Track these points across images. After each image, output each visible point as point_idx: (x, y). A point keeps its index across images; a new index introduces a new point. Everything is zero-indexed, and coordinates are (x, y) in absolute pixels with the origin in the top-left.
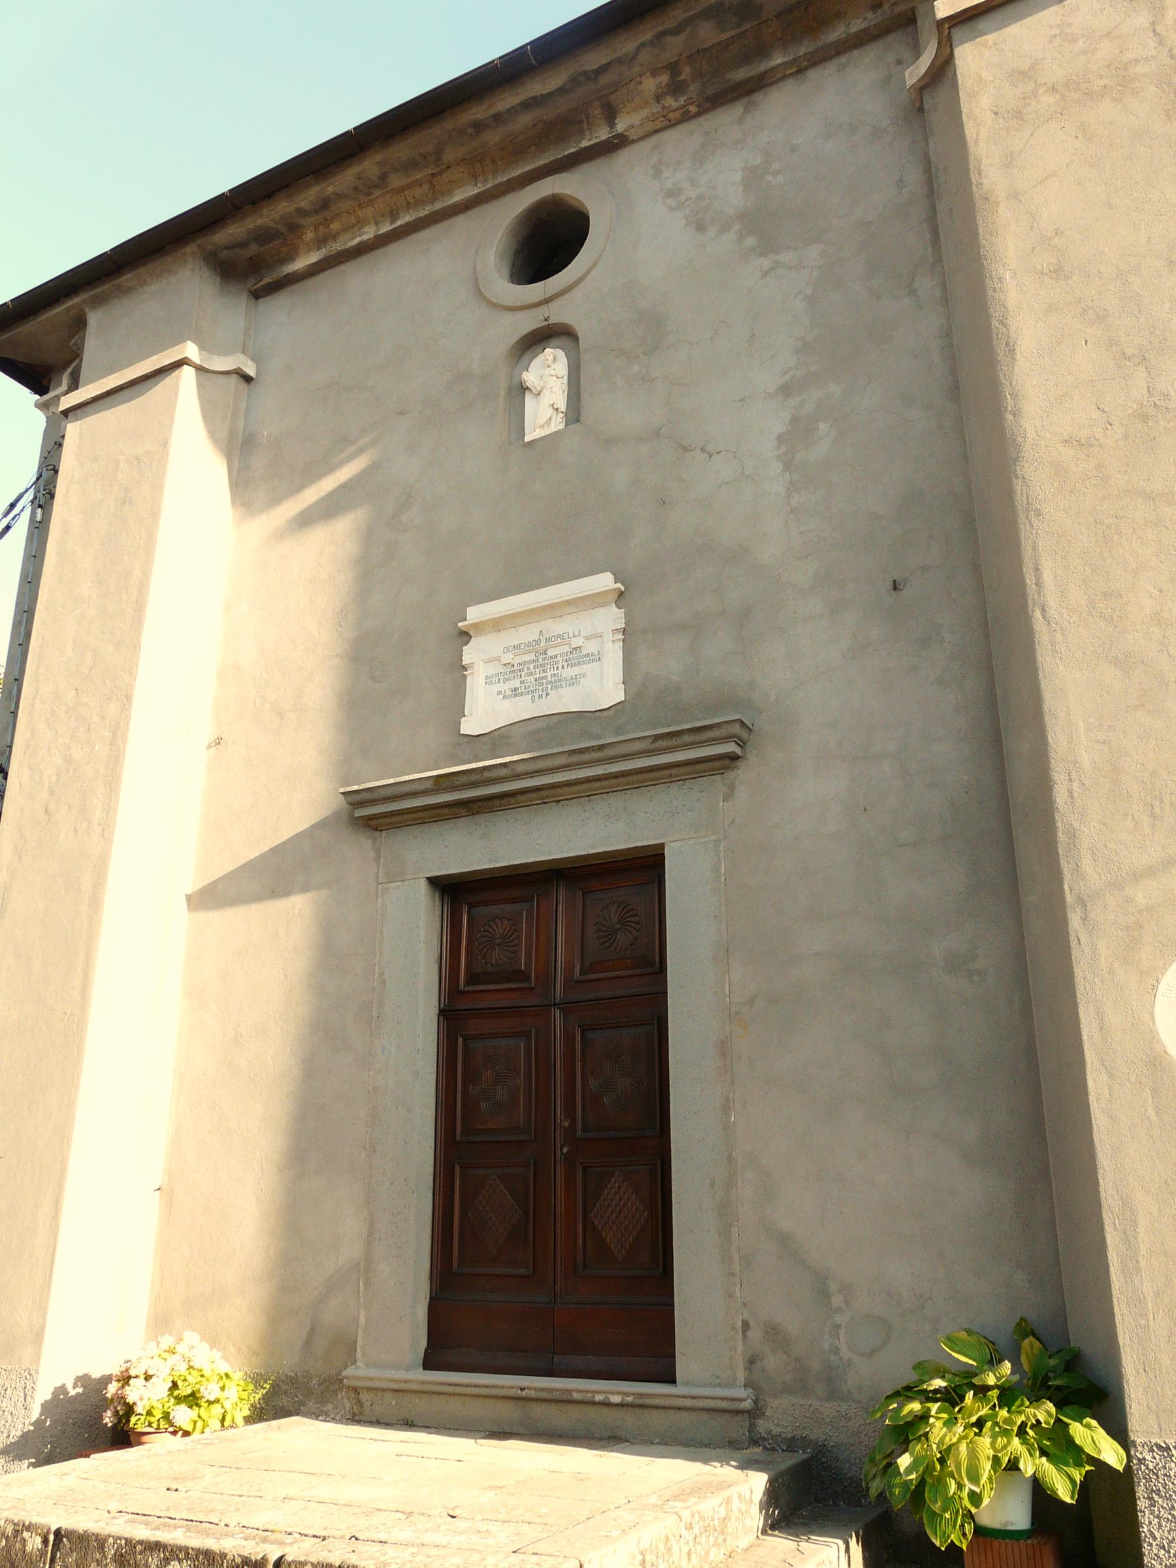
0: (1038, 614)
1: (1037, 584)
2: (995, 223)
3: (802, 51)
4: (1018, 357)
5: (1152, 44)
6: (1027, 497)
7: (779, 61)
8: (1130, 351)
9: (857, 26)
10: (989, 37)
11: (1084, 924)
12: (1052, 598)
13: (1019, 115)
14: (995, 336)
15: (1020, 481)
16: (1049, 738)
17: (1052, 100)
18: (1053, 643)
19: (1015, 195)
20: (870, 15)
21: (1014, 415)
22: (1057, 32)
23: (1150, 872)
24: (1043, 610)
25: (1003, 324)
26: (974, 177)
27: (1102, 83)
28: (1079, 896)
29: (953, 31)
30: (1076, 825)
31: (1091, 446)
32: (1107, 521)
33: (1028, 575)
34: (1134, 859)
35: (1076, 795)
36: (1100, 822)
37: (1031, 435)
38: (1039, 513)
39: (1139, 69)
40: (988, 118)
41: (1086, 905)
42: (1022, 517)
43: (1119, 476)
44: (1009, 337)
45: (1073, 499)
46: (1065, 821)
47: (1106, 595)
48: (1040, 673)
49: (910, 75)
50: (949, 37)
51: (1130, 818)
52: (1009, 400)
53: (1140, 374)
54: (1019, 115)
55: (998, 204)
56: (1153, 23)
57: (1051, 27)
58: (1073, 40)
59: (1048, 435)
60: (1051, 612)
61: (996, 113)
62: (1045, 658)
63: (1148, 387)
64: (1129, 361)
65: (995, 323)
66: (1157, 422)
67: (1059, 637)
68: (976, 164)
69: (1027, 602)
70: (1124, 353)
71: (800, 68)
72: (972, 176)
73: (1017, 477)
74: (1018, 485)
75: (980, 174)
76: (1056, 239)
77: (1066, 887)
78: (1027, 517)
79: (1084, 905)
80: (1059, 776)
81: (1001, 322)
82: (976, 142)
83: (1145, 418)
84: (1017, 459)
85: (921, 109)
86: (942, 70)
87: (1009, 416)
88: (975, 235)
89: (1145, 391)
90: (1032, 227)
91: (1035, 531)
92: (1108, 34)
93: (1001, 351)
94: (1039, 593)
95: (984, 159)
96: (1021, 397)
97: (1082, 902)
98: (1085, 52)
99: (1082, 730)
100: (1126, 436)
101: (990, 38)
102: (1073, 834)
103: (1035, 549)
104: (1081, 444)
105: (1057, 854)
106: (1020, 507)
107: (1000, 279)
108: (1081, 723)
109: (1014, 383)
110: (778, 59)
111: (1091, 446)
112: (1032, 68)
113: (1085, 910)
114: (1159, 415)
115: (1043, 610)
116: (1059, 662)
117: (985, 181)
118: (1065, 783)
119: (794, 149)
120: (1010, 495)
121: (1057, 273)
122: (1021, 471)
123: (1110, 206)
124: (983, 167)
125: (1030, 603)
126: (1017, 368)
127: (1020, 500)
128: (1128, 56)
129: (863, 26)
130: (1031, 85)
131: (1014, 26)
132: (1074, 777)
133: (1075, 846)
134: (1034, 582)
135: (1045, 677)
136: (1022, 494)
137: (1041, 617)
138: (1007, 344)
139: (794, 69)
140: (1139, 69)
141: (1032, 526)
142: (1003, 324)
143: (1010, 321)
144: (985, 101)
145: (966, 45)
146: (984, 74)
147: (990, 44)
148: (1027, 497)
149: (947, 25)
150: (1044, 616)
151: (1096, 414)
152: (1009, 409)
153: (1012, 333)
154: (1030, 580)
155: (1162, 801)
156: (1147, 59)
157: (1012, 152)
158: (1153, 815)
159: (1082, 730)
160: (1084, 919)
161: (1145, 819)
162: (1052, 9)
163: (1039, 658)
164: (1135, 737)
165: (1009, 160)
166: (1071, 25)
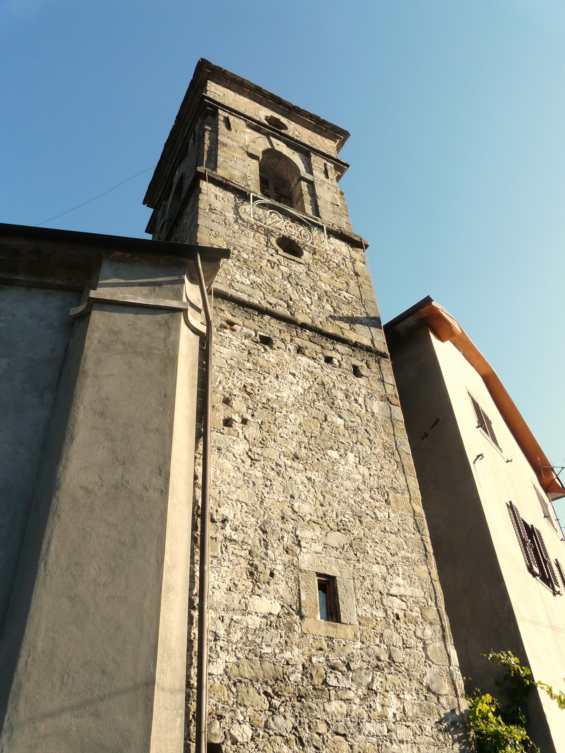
0: (42, 565)
1: (47, 550)
2: (84, 384)
3: (33, 279)
4: (74, 443)
5: (163, 345)
6: (57, 507)
7: (21, 278)
8: (120, 458)
9: (59, 282)
10: (106, 313)
11: (8, 742)
12: (51, 559)
13: (107, 347)
14: (67, 430)
15: (56, 499)
16: (26, 631)
17: (121, 347)
18: (44, 581)
19: (96, 376)
20: (65, 281)
21: (64, 468)
22: (132, 324)
23: (52, 715)
24: (45, 564)
25: (73, 427)
26: (82, 362)
27: (141, 350)
28: (11, 724)
29: (94, 304)
30: (23, 682)
31: (91, 493)
32: (87, 529)
33: (44, 545)
34: (46, 706)
35: (29, 665)
36: (36, 682)
37: (67, 480)
38: (59, 516)
39: (155, 351)
40: (96, 342)
41: (13, 730)
42: (51, 516)
43: (99, 511)
44: (73, 433)
45: (76, 514)
46: (19, 678)
47: (76, 564)
48: (33, 595)
49: (73, 311)
50: (92, 305)
51: (51, 682)
52: (64, 460)
53: (120, 469)
54: (107, 347)
55: (88, 377)
56: (165, 338)
57: (130, 321)
58: (136, 329)
59: (75, 482)
60: (49, 566)
61: (99, 342)
62: (38, 589)
63: (122, 476)
64: (118, 462)
65: (70, 425)
66: (121, 492)
67: (48, 578)
68: (85, 357)
69: (39, 557)
70: (117, 458)
71: (29, 286)
72: (82, 361)
73: (55, 497)
74: (54, 501)
75: (85, 362)
76: (106, 401)
77: (6, 718)
78: (53, 517)
79: (12, 730)
80: (24, 653)
81: (72, 425)
82: (88, 349)
83: (116, 488)
84: (57, 488)
85: (72, 325)
86: (85, 316)
87: (61, 468)
88: (74, 385)
89: (120, 477)
90: (98, 392)
91: (54, 524)
92: (149, 334)
93: (68, 438)
94: (46, 555)
95: (89, 358)
96: (69, 461)
97: (12, 728)
98: (139, 336)
99: (43, 630)
100: (107, 494)
101: (107, 313)
102: (20, 686)
103: (52, 532)
104: (88, 491)
105: (9, 697)
106: (51, 511)
107: (78, 408)
108: (44, 626)
109: (68, 454)
110: (21, 278)
111: (91, 493)
112: (118, 332)
113: (12, 732)
114: (123, 490)
115: (45, 564)
116: (44, 592)
117: (86, 366)
118: (25, 657)
119: (13, 315)
120: (50, 503)
121: (102, 414)
122: (58, 494)
123: (130, 397)
124: (87, 360)
125: (40, 558)
126: (72, 448)
127: (53, 508)
128: (153, 345)
129: (61, 283)
130: (116, 338)
131: (117, 314)
132: (31, 655)
133: (19, 694)
134: (46, 548)
135: (35, 597)
136: (54, 505)
137: (43, 567)
138: (71, 436)
139: (27, 285)
140: (155, 351)
141: (54, 521)
142: (73, 427)
143: (76, 426)
144: (97, 335)
145: (97, 312)
146: (100, 325)
147: (106, 315)
148: (57, 507)
149: (92, 301)
150: (44, 567)
151: (97, 480)
152: (63, 464)
153: (75, 432)
154: (44, 547)
155: (69, 675)
156: (159, 349)
157: (100, 360)
158: (62, 683)
159: (43, 630)
160: (9, 739)
161: (58, 683)
162: (132, 315)
163: (35, 588)
164: (67, 639)
165: (98, 362)
166: (137, 324)
